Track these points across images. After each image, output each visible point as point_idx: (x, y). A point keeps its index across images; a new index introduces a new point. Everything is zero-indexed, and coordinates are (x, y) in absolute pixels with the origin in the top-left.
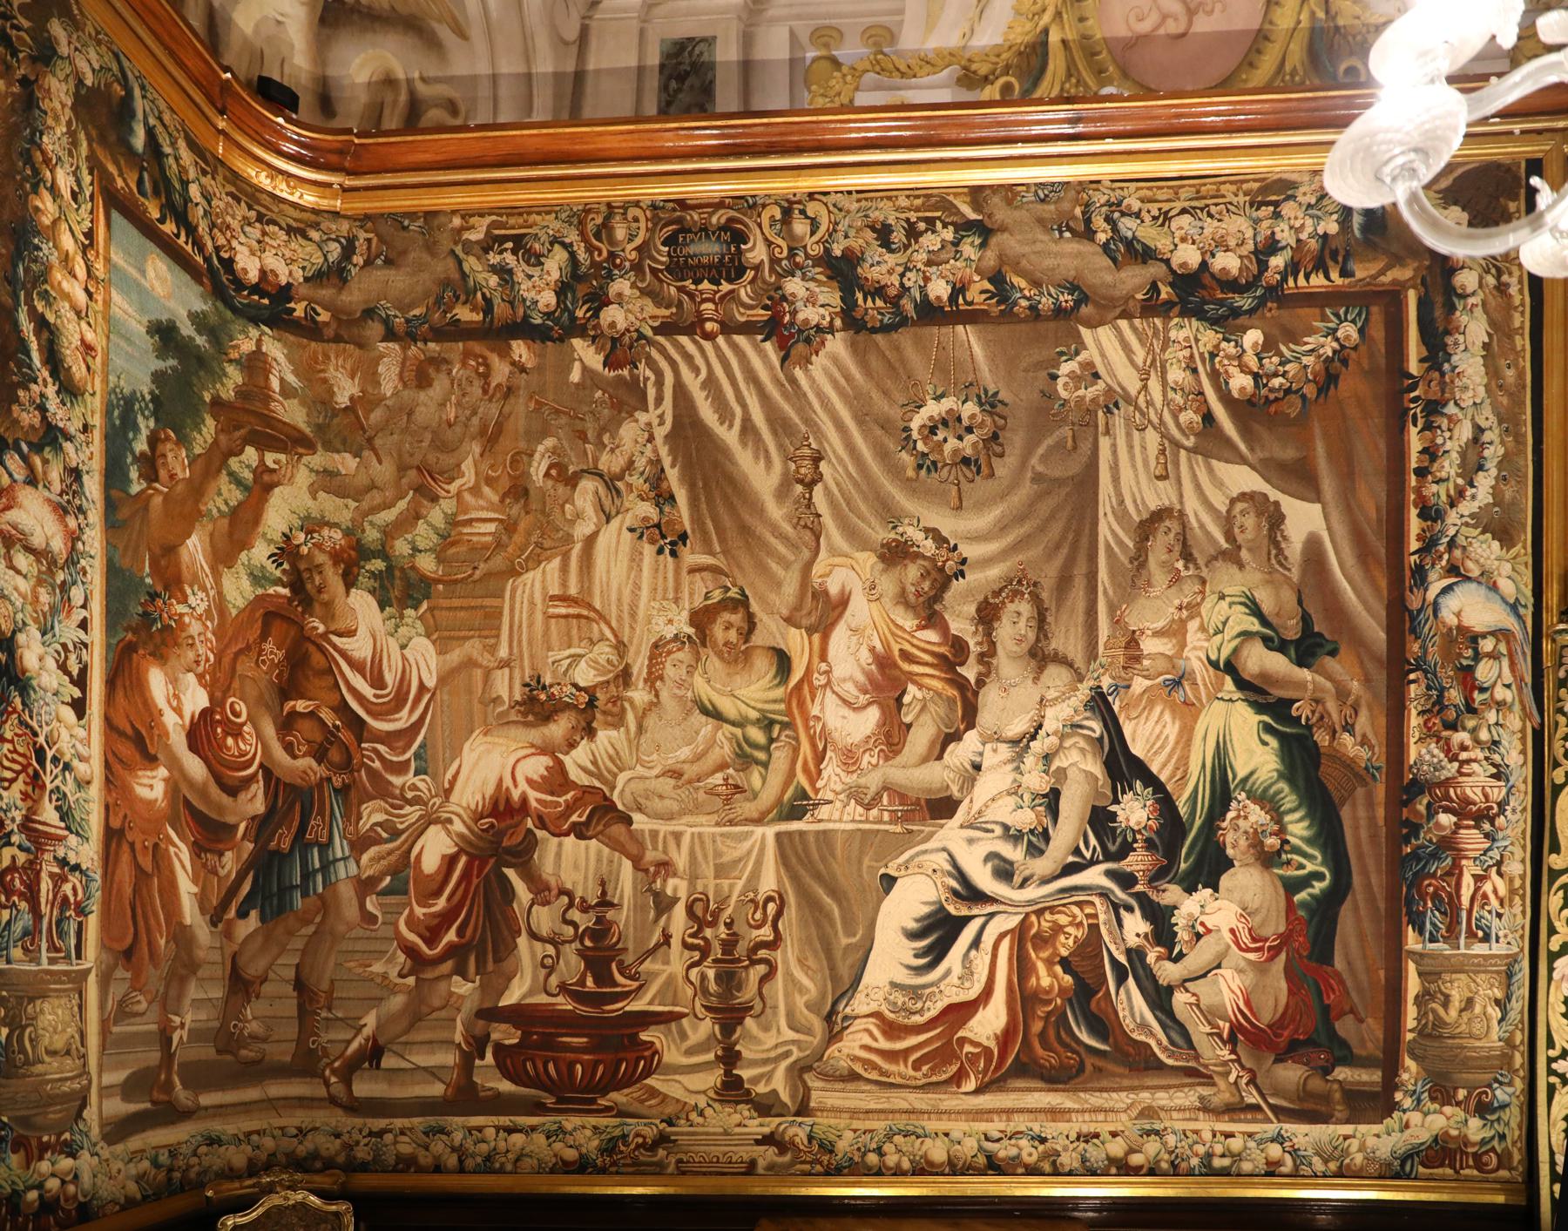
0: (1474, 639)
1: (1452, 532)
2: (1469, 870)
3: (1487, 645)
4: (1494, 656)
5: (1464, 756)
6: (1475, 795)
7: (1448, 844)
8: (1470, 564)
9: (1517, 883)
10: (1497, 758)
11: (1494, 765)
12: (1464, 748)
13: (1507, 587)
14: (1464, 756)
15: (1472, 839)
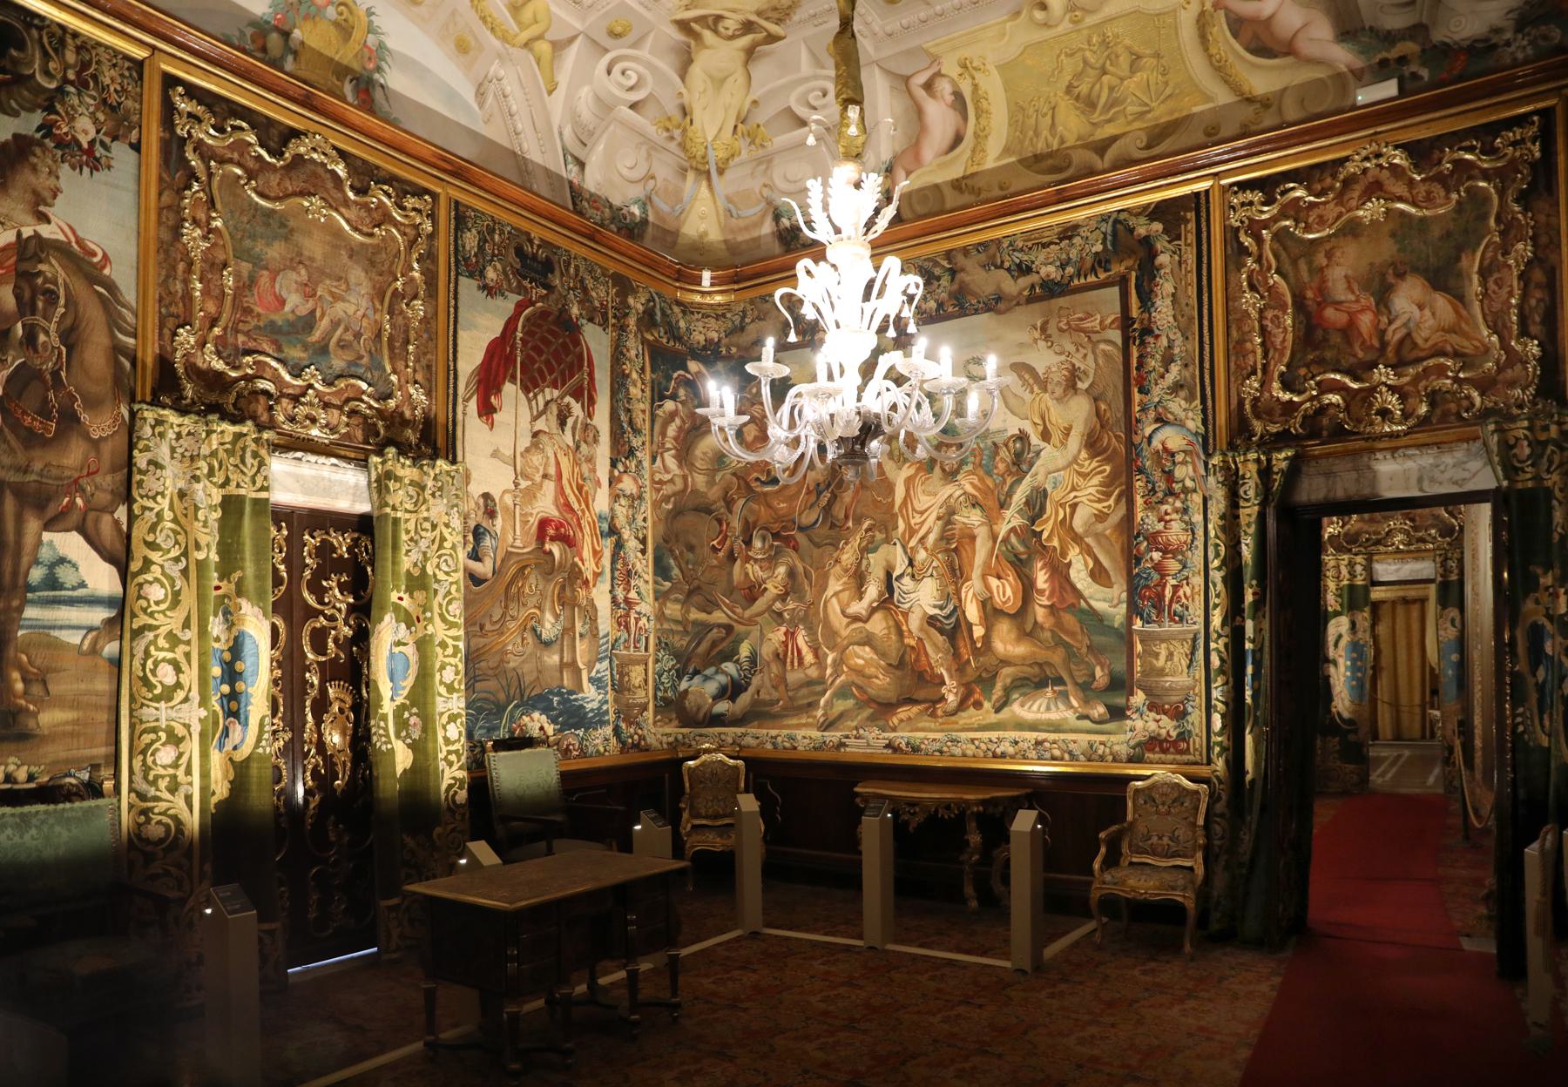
0: (1173, 455)
1: (1157, 400)
2: (1172, 582)
3: (1179, 458)
4: (1184, 463)
5: (1168, 518)
6: (1173, 539)
7: (1158, 567)
8: (1169, 416)
9: (1197, 590)
10: (1186, 518)
11: (1186, 523)
12: (1166, 514)
13: (1191, 425)
14: (1168, 518)
15: (1173, 565)
